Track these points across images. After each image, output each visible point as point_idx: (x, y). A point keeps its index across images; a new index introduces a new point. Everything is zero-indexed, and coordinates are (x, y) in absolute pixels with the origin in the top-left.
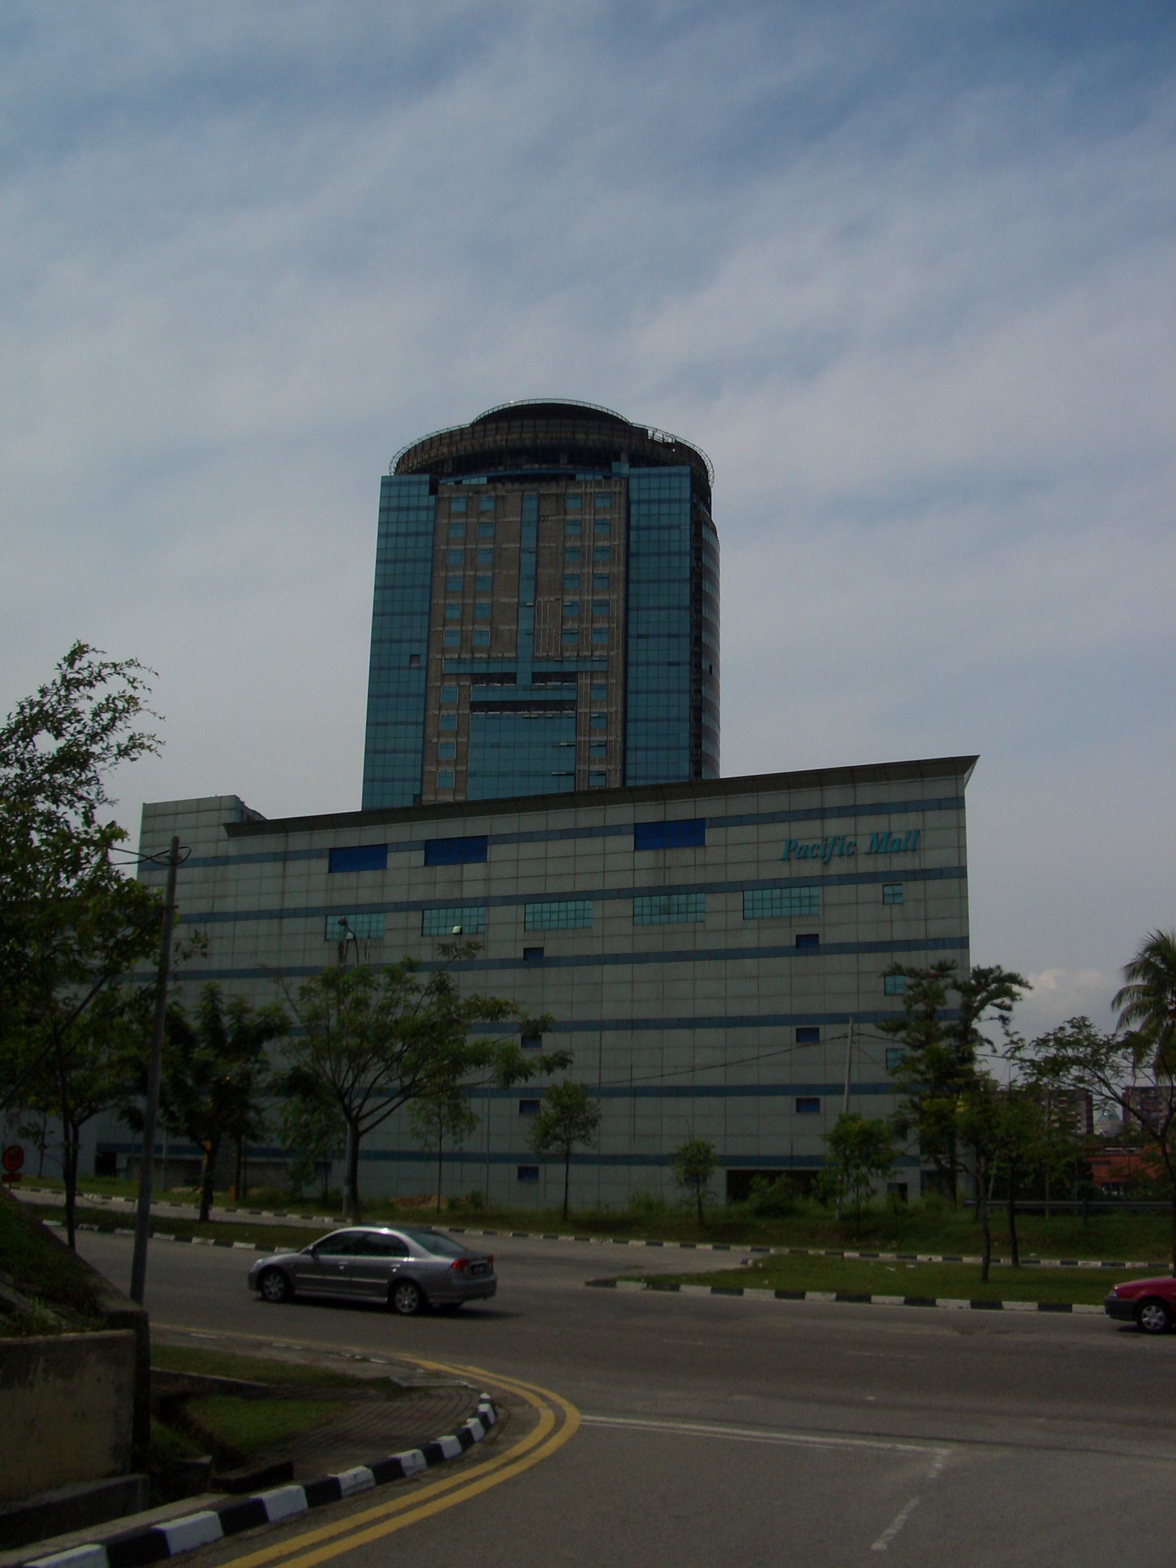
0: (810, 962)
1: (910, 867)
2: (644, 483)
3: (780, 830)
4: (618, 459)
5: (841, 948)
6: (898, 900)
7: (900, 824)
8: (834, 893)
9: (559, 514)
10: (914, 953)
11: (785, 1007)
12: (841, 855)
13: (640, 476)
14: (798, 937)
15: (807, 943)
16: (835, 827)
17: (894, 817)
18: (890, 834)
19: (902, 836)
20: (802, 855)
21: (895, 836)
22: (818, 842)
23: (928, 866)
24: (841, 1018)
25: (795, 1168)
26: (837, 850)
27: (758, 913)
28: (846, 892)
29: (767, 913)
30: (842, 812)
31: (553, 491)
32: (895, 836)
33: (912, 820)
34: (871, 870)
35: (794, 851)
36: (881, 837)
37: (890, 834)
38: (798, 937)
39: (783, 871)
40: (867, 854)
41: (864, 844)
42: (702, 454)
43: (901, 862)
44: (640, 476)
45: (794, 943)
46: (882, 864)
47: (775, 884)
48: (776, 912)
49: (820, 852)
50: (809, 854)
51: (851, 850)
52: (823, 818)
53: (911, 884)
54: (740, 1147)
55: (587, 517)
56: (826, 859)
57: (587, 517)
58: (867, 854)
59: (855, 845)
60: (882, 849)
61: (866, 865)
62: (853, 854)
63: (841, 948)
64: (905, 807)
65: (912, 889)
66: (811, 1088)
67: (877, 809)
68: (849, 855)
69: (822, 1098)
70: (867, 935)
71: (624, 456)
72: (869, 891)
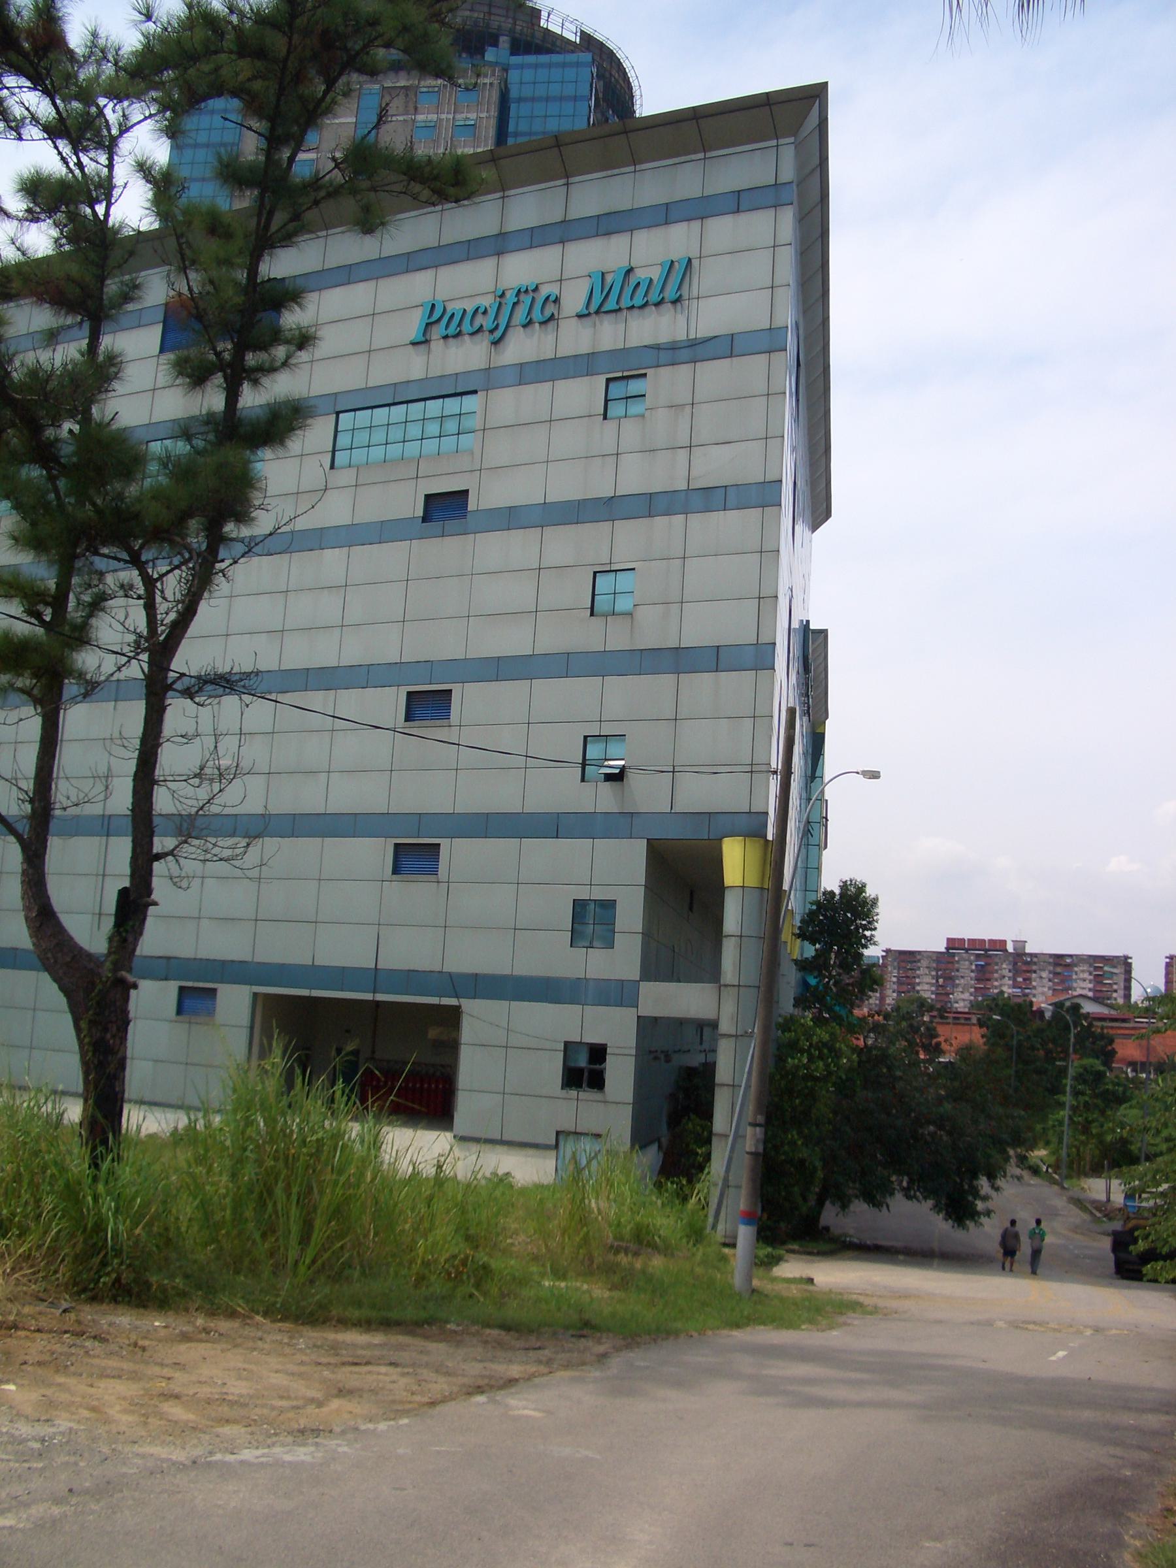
0: (444, 550)
1: (664, 338)
2: (528, 75)
3: (419, 287)
4: (495, 44)
5: (510, 518)
6: (635, 408)
7: (649, 251)
8: (507, 403)
9: (407, 114)
10: (660, 521)
11: (386, 647)
12: (528, 324)
13: (521, 67)
14: (428, 497)
15: (445, 508)
16: (521, 269)
17: (641, 236)
18: (630, 271)
19: (656, 274)
20: (452, 330)
21: (641, 274)
22: (487, 301)
23: (703, 333)
24: (499, 669)
25: (380, 997)
26: (520, 315)
27: (359, 456)
28: (532, 399)
29: (377, 453)
30: (536, 237)
31: (402, 83)
32: (641, 274)
33: (678, 240)
34: (584, 349)
35: (440, 324)
36: (609, 279)
37: (630, 271)
38: (428, 497)
39: (414, 367)
40: (580, 316)
41: (574, 299)
42: (626, 65)
43: (647, 329)
44: (521, 67)
45: (420, 512)
46: (609, 335)
47: (397, 396)
48: (394, 450)
49: (488, 323)
50: (466, 327)
51: (550, 309)
52: (499, 254)
53: (665, 372)
54: (282, 947)
55: (444, 116)
56: (498, 334)
57: (444, 116)
58: (580, 316)
59: (557, 300)
60: (611, 304)
61: (575, 338)
62: (552, 317)
63: (510, 518)
64: (666, 214)
65: (665, 384)
66: (420, 819)
67: (607, 225)
68: (544, 323)
69: (444, 843)
70: (566, 486)
71: (504, 42)
72: (584, 393)
